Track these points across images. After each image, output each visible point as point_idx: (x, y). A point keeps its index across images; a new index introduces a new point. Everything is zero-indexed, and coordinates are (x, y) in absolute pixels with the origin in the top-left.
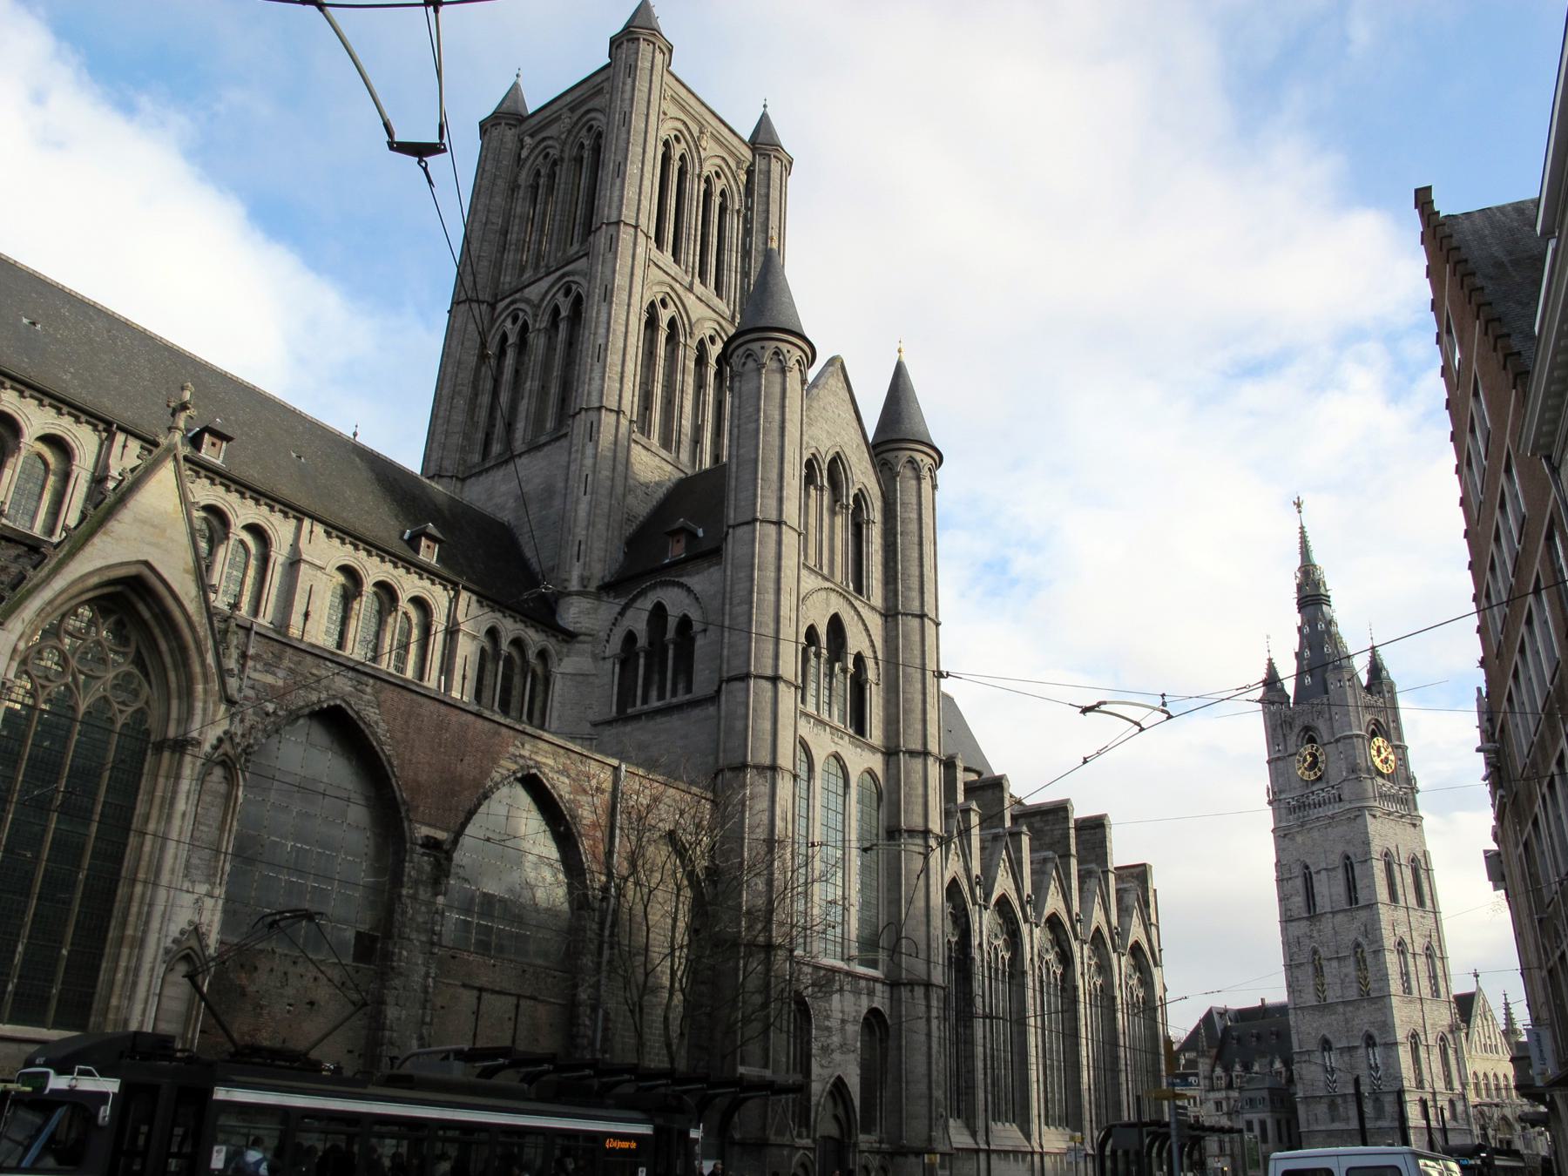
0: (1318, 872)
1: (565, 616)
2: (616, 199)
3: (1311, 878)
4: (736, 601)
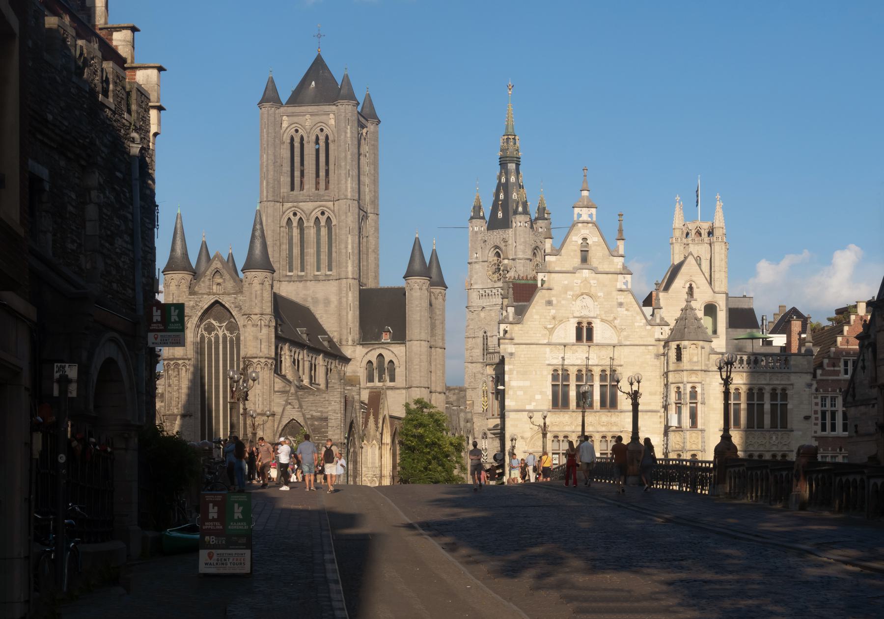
0: (490, 337)
1: (347, 352)
2: (349, 188)
3: (487, 339)
4: (415, 364)
